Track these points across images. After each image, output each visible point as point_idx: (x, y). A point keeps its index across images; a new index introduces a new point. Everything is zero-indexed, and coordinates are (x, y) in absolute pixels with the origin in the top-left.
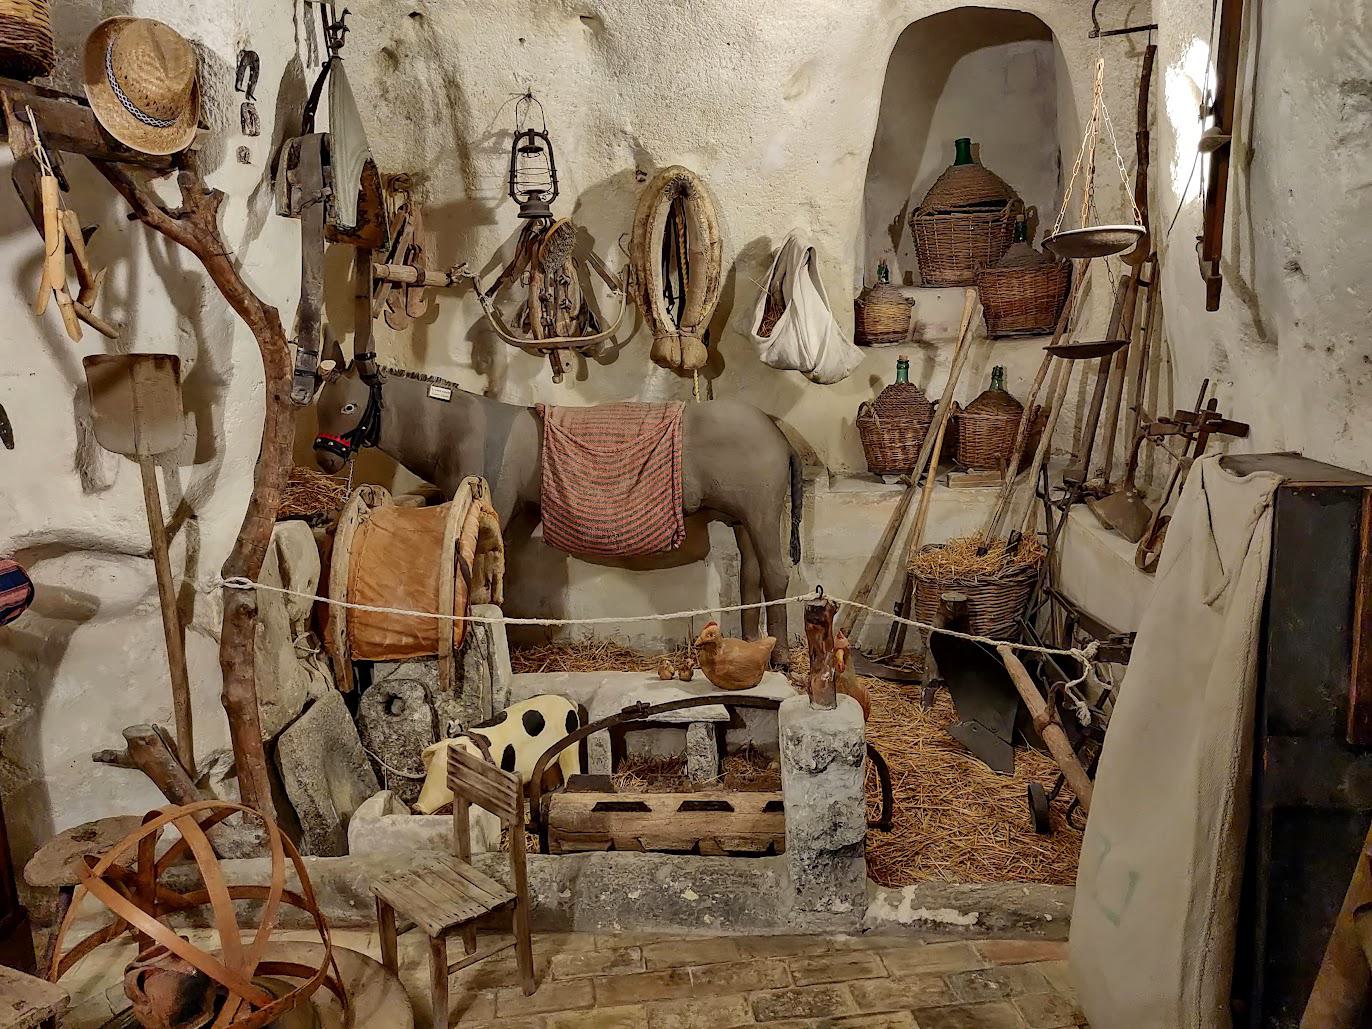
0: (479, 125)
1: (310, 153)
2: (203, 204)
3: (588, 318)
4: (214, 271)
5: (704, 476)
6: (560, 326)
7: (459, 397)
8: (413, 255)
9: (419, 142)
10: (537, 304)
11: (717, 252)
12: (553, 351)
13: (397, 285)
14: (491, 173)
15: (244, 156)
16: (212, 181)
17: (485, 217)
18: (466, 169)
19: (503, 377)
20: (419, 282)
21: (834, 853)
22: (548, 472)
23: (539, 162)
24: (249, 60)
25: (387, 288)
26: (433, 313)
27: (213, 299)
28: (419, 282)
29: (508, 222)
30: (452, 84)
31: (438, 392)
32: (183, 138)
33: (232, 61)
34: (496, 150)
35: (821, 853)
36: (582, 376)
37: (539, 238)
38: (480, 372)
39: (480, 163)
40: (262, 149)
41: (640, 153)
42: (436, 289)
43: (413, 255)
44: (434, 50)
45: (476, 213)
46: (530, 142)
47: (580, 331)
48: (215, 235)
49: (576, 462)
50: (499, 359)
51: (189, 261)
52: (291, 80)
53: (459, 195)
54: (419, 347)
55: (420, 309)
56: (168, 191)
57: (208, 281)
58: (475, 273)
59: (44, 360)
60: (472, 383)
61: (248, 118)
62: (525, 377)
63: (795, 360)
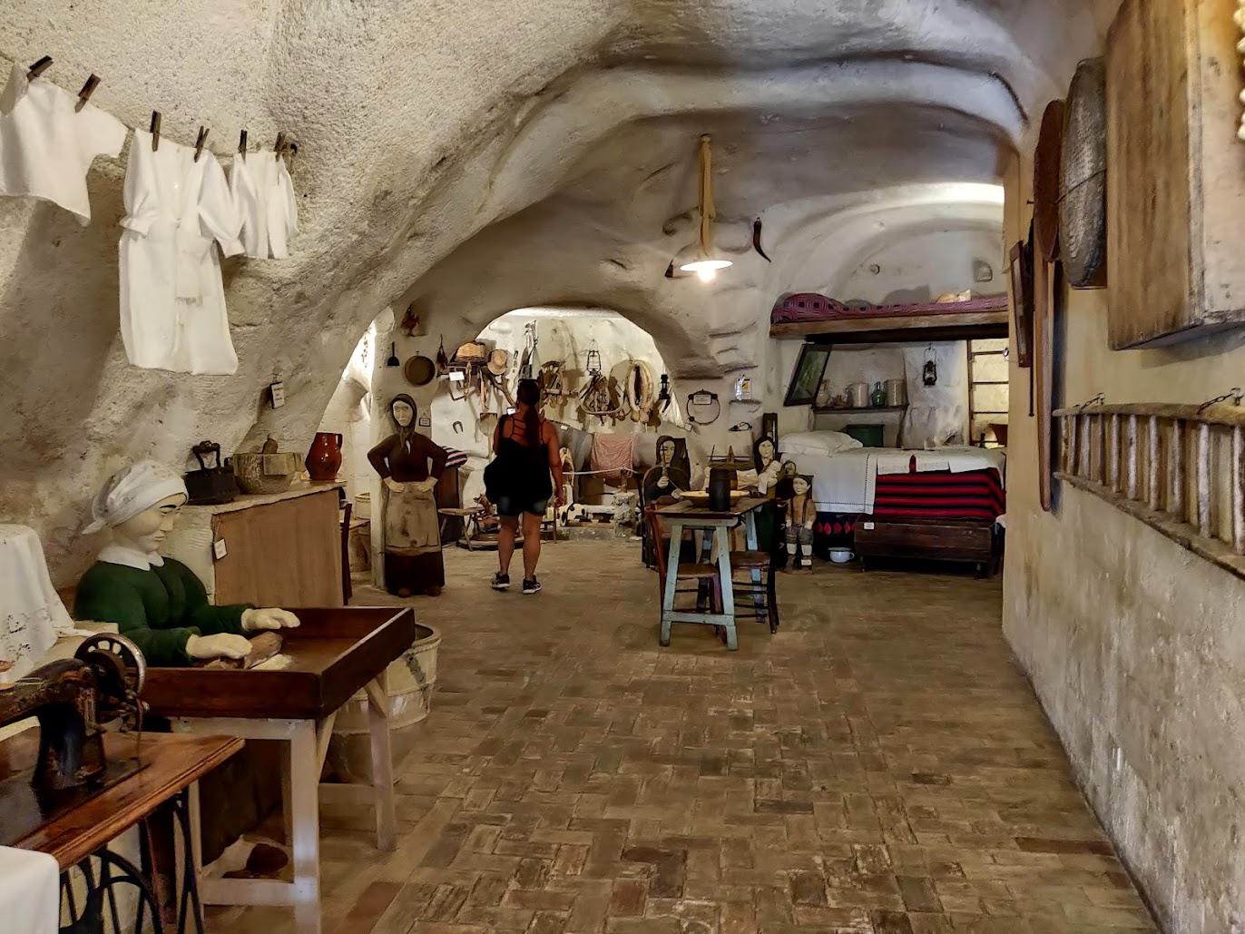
0: (579, 348)
1: (527, 370)
2: (505, 381)
3: (613, 405)
4: (506, 396)
5: (640, 455)
6: (602, 408)
7: (570, 429)
8: (559, 386)
9: (563, 352)
10: (596, 401)
11: (651, 386)
12: (601, 416)
13: (553, 395)
14: (583, 361)
15: (514, 371)
16: (507, 377)
17: (582, 374)
18: (577, 361)
19: (588, 425)
20: (560, 394)
21: (623, 524)
22: (593, 453)
23: (596, 359)
24: (517, 352)
25: (550, 396)
26: (565, 403)
27: (505, 400)
28: (560, 394)
29: (588, 378)
30: (572, 337)
31: (563, 427)
32: (503, 370)
33: (513, 353)
34: (585, 355)
35: (620, 524)
36: (614, 424)
37: (597, 381)
38: (580, 422)
39: (580, 358)
40: (517, 369)
41: (630, 355)
42: (566, 396)
43: (559, 386)
44: (567, 329)
45: (577, 373)
46: (593, 353)
47: (609, 409)
48: (507, 388)
49: (602, 449)
50: (587, 419)
51: (501, 393)
52: (526, 352)
53: (574, 367)
54: (561, 414)
55: (561, 401)
56: (499, 380)
57: (504, 397)
58: (578, 391)
59: (470, 412)
60: (579, 426)
61: (515, 363)
62: (595, 424)
63: (672, 421)
